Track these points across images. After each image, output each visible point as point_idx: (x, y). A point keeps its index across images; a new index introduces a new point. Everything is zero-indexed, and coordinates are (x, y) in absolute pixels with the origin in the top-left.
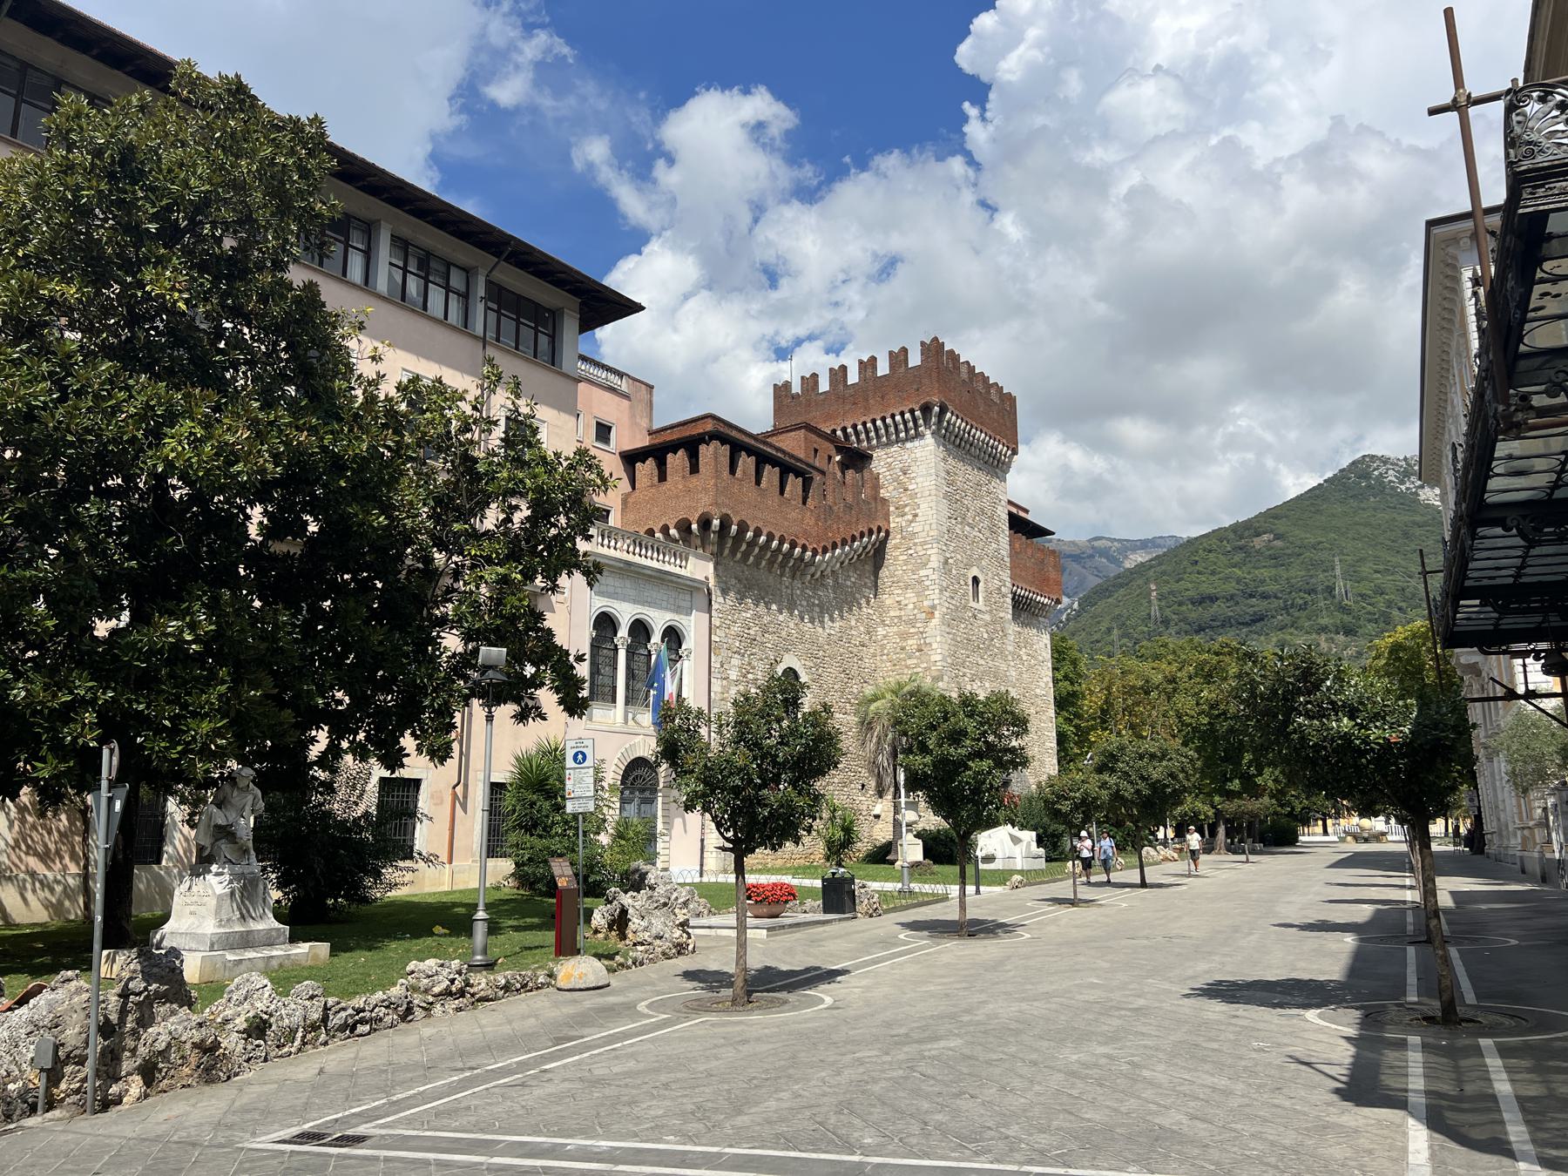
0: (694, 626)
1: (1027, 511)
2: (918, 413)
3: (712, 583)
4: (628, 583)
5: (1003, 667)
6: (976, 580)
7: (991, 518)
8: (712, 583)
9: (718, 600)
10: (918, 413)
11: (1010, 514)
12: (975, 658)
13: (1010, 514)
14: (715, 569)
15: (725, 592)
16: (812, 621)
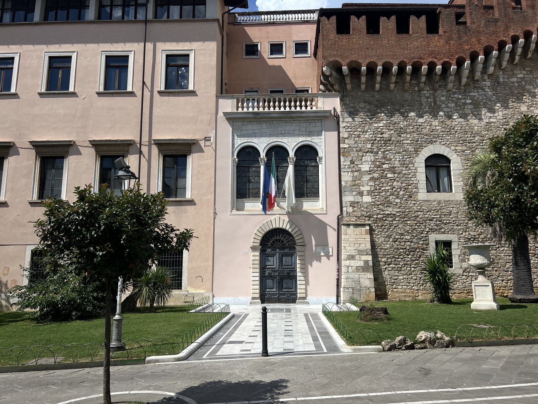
0: (325, 144)
3: (339, 110)
4: (264, 126)
8: (339, 110)
9: (346, 121)
14: (341, 100)
15: (353, 114)
16: (464, 116)
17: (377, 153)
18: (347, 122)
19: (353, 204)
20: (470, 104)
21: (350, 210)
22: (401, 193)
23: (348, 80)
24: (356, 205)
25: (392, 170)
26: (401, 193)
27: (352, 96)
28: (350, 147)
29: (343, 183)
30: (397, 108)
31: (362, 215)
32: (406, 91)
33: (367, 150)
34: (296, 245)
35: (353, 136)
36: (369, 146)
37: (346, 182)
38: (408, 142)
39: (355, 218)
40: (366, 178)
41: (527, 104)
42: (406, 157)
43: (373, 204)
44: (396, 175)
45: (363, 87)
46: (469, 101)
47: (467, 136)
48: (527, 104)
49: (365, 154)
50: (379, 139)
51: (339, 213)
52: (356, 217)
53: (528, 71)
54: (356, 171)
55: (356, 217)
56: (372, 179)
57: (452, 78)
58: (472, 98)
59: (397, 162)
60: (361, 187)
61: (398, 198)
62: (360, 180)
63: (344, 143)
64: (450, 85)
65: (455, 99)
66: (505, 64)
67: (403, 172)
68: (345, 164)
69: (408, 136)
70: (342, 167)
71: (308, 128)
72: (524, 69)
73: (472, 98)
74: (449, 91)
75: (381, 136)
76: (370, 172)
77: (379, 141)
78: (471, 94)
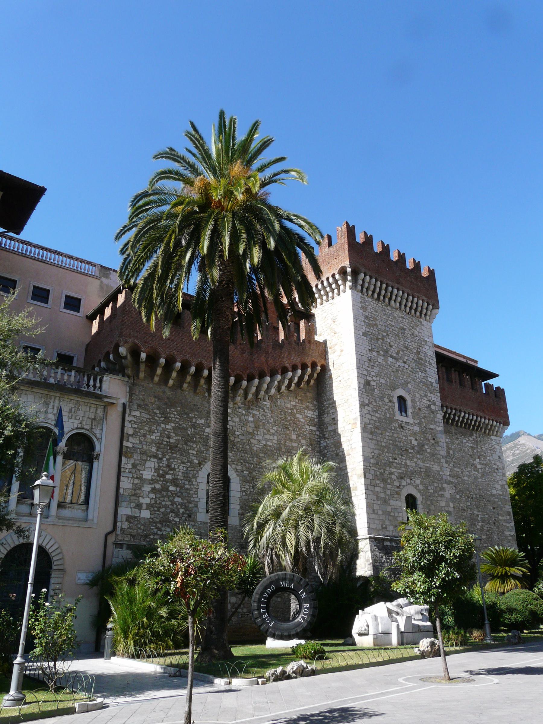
1: (476, 362)
2: (337, 277)
5: (436, 468)
6: (402, 400)
7: (418, 353)
10: (337, 277)
11: (436, 352)
12: (403, 460)
13: (436, 352)
17: (161, 459)
18: (134, 416)
19: (129, 518)
20: (251, 422)
21: (126, 525)
22: (181, 511)
23: (142, 367)
24: (132, 521)
25: (175, 482)
26: (181, 511)
27: (143, 387)
28: (133, 447)
29: (121, 491)
30: (186, 411)
31: (138, 534)
32: (198, 394)
33: (152, 454)
34: (51, 568)
35: (139, 434)
36: (154, 449)
37: (125, 489)
38: (194, 452)
39: (129, 536)
40: (147, 488)
41: (296, 433)
42: (190, 469)
43: (151, 521)
44: (178, 489)
45: (156, 379)
46: (251, 419)
47: (246, 455)
48: (296, 433)
49: (149, 458)
50: (165, 443)
51: (110, 528)
52: (131, 535)
53: (299, 400)
54: (137, 478)
55: (131, 535)
56: (153, 490)
57: (241, 392)
58: (254, 416)
59: (180, 474)
60: (140, 498)
61: (177, 516)
62: (140, 489)
63: (128, 441)
64: (238, 399)
65: (239, 414)
66: (283, 388)
67: (186, 486)
68: (126, 466)
69: (195, 446)
70: (122, 470)
71: (87, 414)
72: (296, 398)
73: (254, 416)
74: (235, 404)
75: (168, 440)
76: (152, 481)
77: (165, 445)
78: (254, 412)
